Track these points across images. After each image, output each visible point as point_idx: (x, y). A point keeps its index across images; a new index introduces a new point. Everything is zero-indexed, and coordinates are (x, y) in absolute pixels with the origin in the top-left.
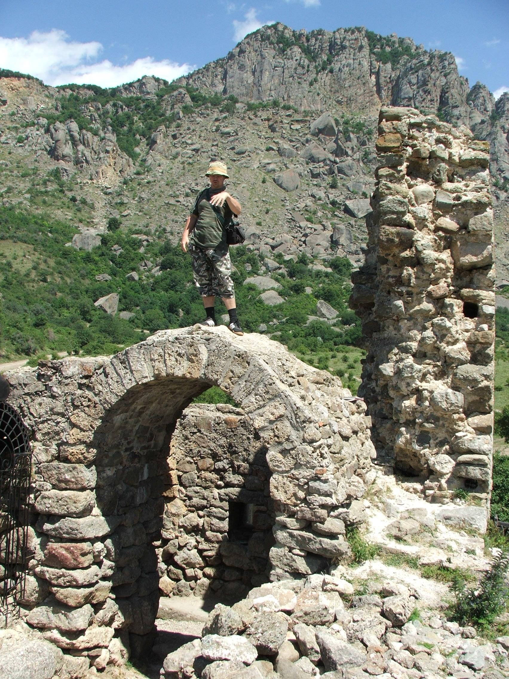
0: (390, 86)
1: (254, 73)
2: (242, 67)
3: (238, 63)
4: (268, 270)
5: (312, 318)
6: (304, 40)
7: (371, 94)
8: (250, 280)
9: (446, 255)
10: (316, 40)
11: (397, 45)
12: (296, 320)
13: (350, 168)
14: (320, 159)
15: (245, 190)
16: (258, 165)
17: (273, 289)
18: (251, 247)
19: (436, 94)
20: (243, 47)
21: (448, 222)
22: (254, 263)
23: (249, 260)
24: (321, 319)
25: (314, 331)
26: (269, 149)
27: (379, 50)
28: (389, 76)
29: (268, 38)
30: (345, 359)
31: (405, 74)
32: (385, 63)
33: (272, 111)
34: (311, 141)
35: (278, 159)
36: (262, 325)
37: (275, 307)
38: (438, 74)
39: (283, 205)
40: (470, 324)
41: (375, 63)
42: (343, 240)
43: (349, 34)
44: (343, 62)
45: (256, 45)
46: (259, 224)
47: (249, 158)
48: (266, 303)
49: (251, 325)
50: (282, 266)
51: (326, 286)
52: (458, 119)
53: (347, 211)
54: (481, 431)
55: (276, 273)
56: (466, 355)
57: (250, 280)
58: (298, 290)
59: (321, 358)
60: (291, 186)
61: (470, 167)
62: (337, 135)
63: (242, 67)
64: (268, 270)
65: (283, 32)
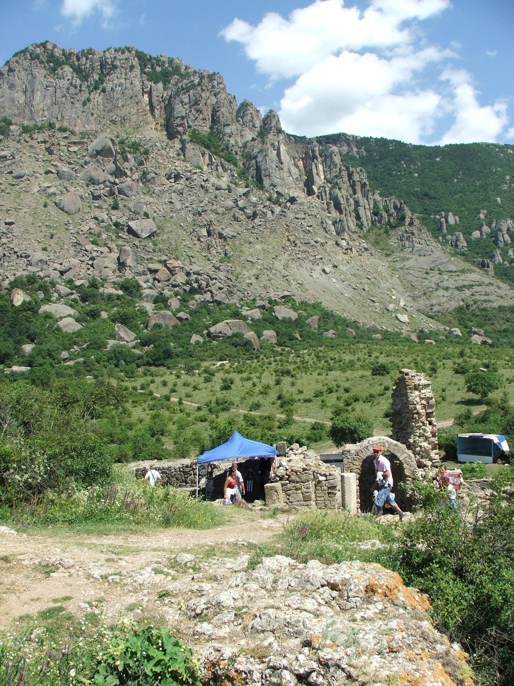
0: (163, 105)
1: (25, 92)
2: (12, 87)
3: (8, 82)
4: (60, 296)
5: (112, 343)
6: (75, 59)
7: (144, 113)
8: (45, 308)
9: (424, 411)
10: (87, 59)
11: (167, 65)
12: (97, 345)
13: (130, 188)
14: (100, 181)
15: (27, 215)
16: (38, 189)
17: (70, 316)
18: (42, 274)
19: (208, 113)
20: (13, 65)
21: (424, 402)
22: (46, 290)
23: (41, 288)
24: (122, 343)
25: (115, 355)
26: (48, 172)
27: (150, 70)
28: (161, 95)
29: (38, 57)
30: (165, 384)
31: (177, 94)
32: (156, 83)
33: (47, 133)
34: (89, 163)
35: (58, 182)
36: (63, 352)
37: (74, 333)
38: (208, 94)
39: (67, 229)
40: (430, 427)
41: (146, 82)
42: (129, 262)
43: (120, 53)
44: (115, 82)
45: (26, 64)
46: (45, 249)
47: (28, 182)
48: (64, 330)
49: (53, 353)
50: (73, 291)
51: (120, 309)
52: (230, 137)
53: (131, 231)
54: (436, 454)
55: (69, 299)
56: (431, 436)
57: (45, 308)
58: (94, 315)
59: (143, 384)
60: (73, 209)
61: (427, 386)
62: (116, 157)
63: (12, 87)
64: (60, 296)
65: (53, 51)
